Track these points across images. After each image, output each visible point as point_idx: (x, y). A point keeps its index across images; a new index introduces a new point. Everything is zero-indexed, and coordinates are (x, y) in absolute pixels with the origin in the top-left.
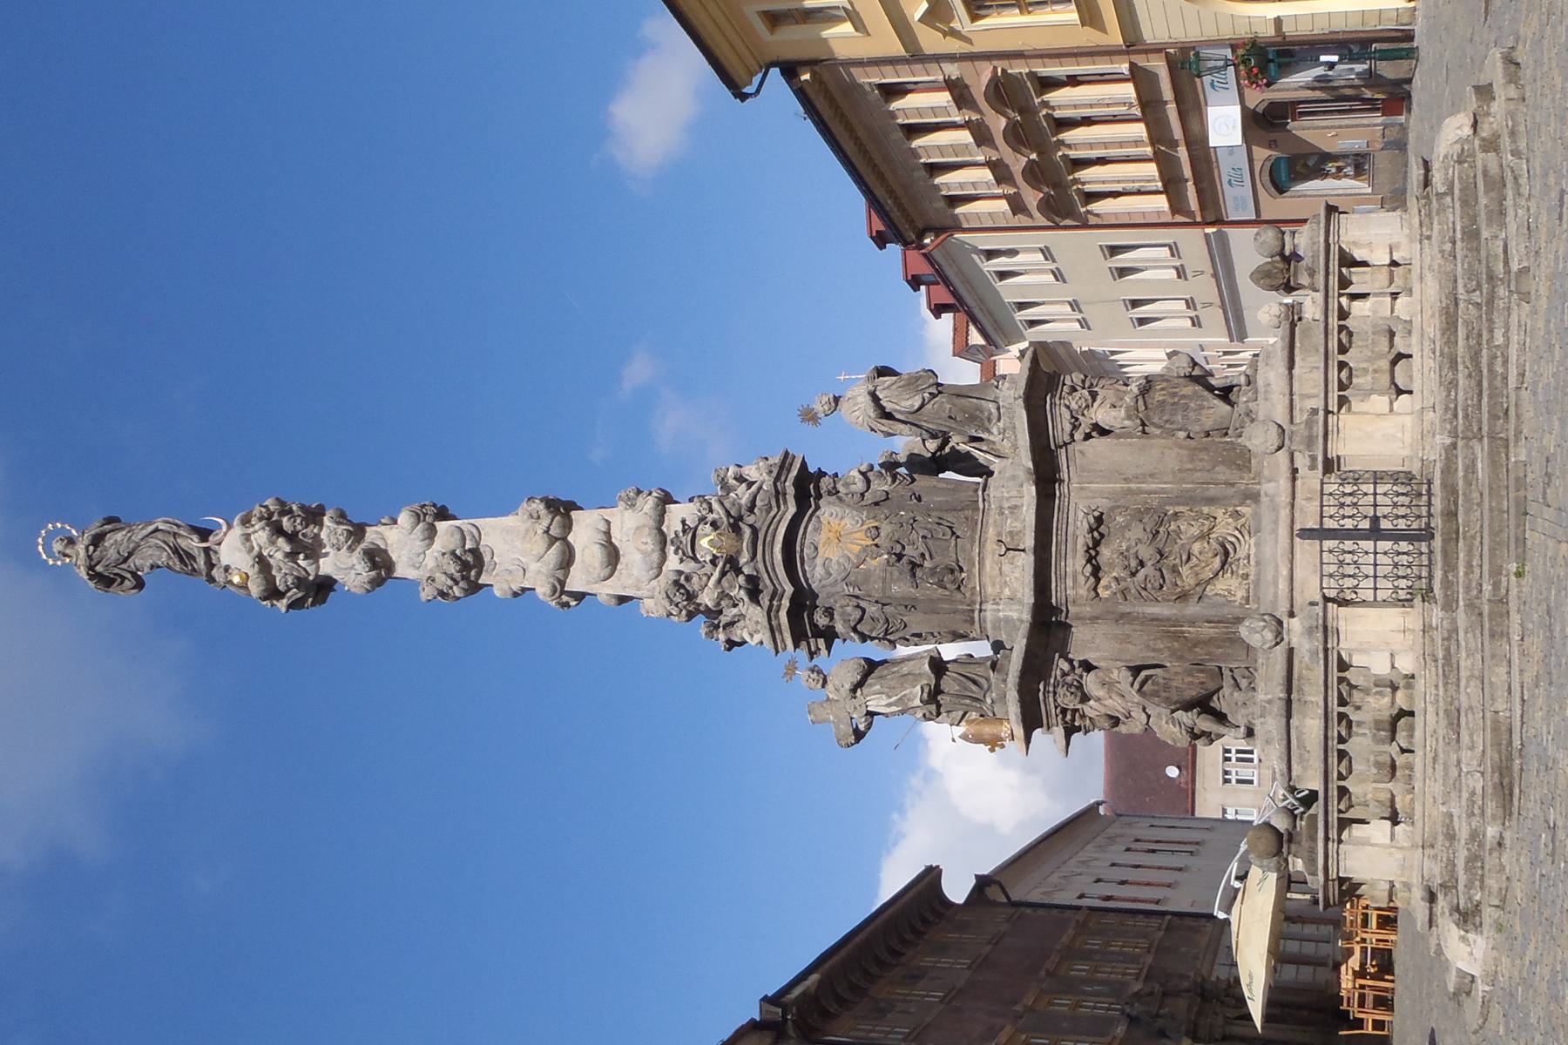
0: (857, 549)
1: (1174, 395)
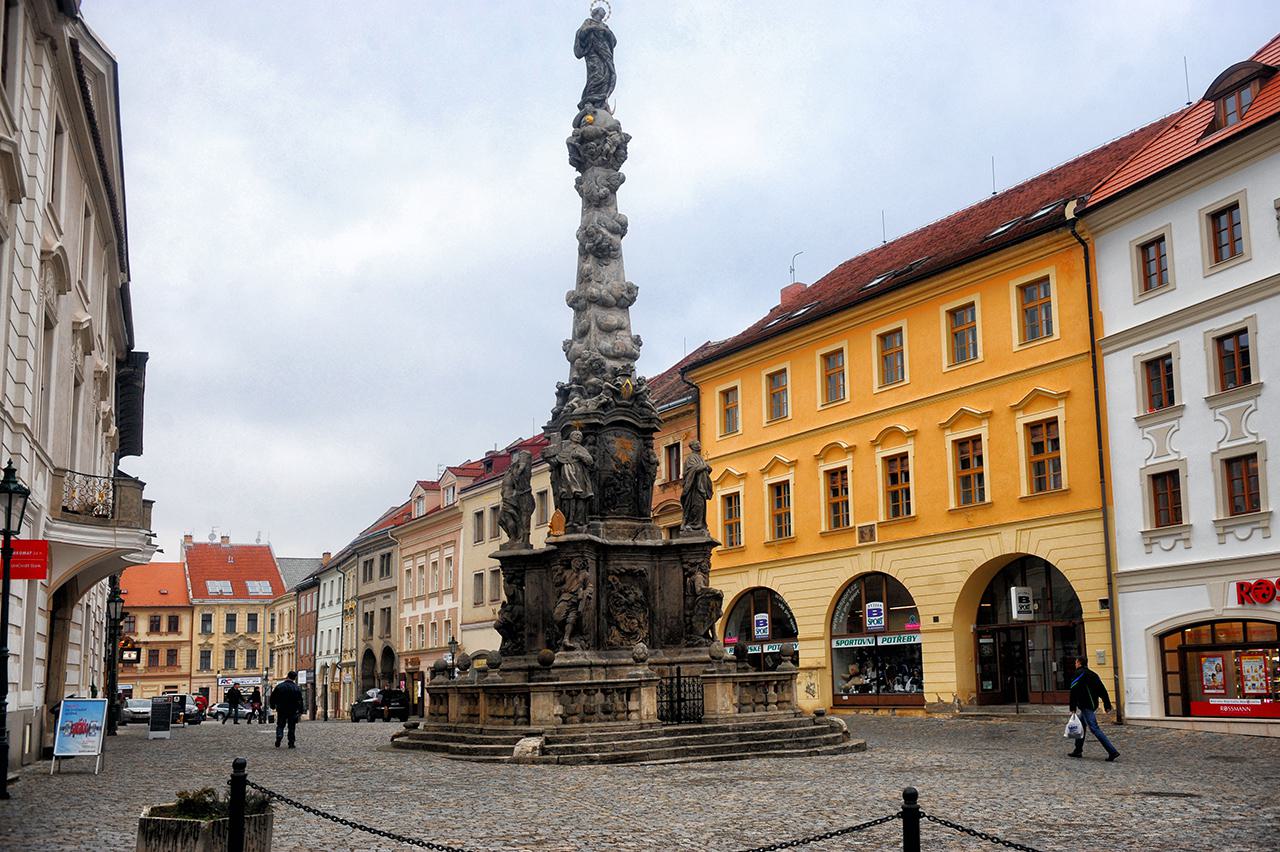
0: (620, 457)
1: (712, 610)
